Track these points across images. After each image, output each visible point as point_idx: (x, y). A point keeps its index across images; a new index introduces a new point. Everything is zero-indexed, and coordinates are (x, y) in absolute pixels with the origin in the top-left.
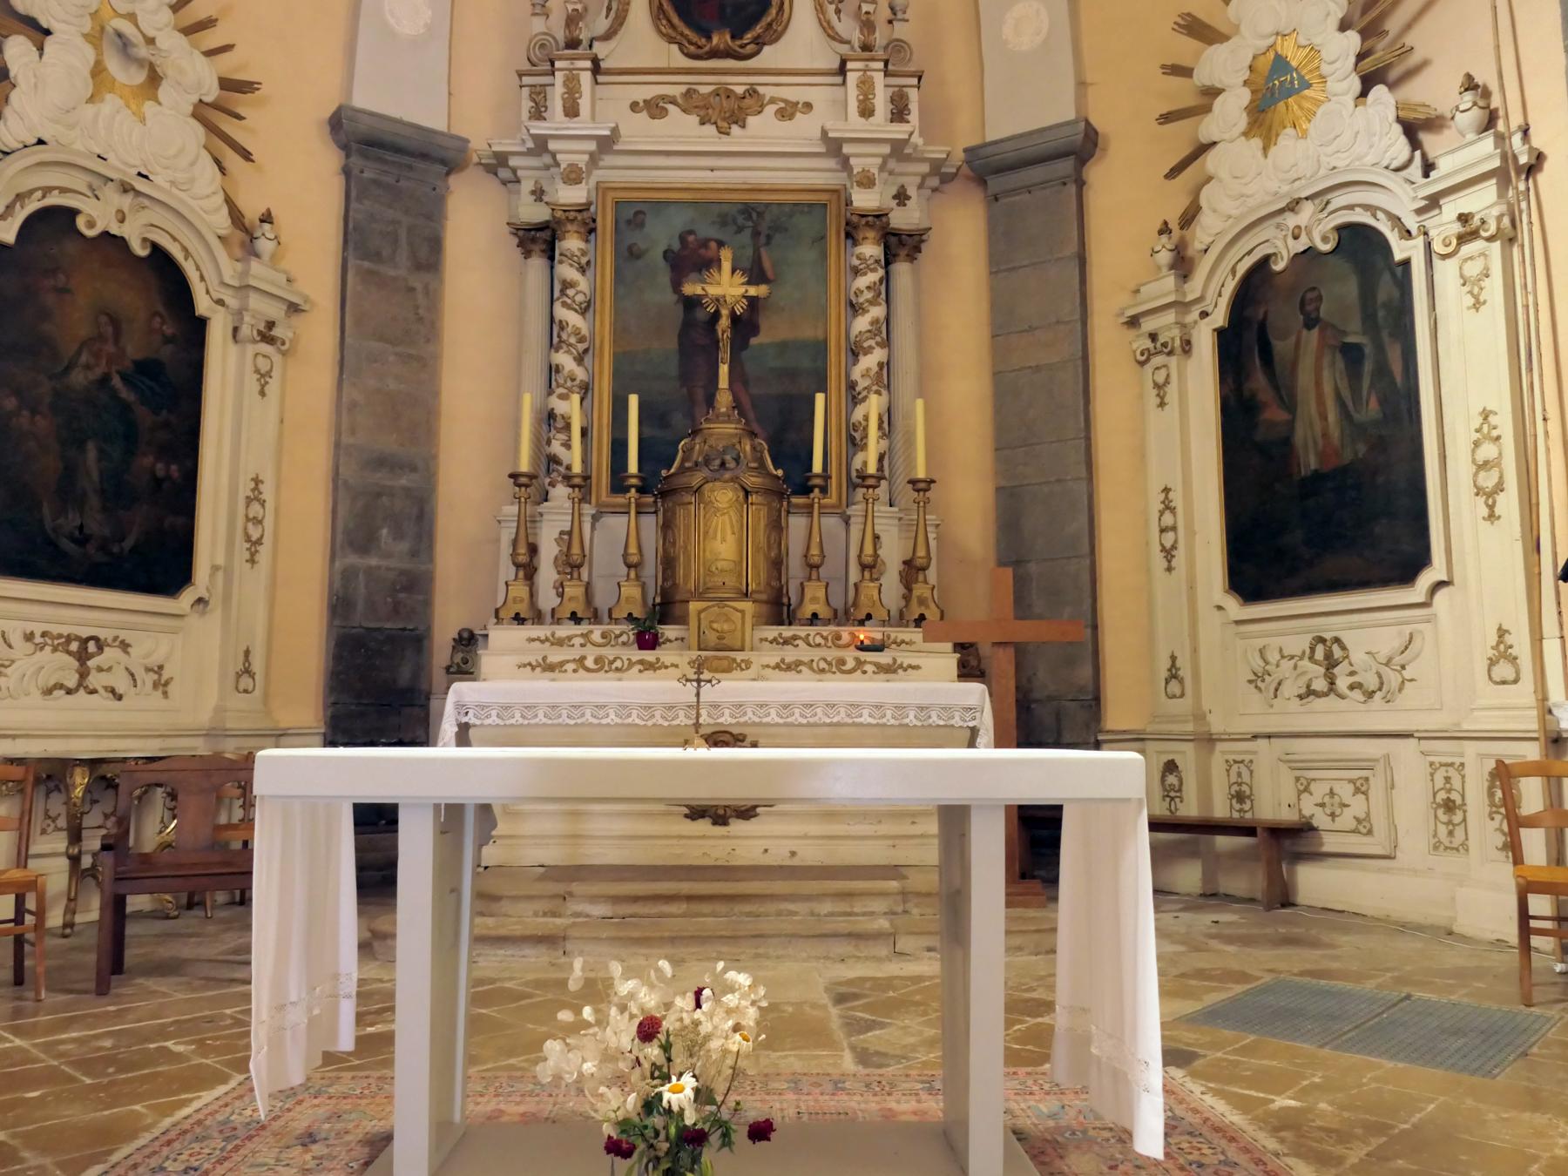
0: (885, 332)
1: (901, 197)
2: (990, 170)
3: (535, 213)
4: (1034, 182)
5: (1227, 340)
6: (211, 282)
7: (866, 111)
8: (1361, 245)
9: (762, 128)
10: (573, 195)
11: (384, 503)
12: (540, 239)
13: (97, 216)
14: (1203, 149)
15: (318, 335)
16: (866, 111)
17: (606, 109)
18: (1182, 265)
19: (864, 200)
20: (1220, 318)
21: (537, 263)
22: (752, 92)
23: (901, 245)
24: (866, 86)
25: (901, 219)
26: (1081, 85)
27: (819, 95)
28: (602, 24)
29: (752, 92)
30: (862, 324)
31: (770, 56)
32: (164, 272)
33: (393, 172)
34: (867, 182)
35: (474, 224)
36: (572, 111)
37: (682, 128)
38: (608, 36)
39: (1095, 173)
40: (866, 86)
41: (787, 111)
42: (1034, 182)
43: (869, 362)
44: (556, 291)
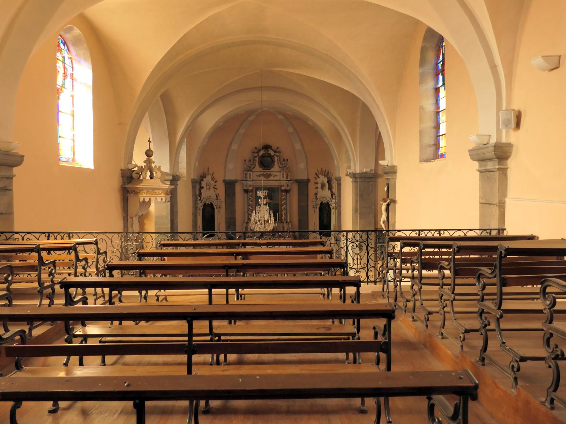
0: (286, 204)
1: (288, 186)
2: (298, 182)
3: (245, 188)
4: (303, 185)
5: (320, 208)
6: (215, 204)
7: (283, 177)
8: (328, 204)
9: (272, 178)
10: (251, 188)
11: (231, 222)
12: (246, 191)
13: (207, 202)
14: (317, 188)
15: (223, 205)
16: (283, 177)
17: (254, 176)
18: (317, 199)
19: (283, 188)
20: (318, 206)
21: (246, 194)
22: (270, 174)
23: (287, 191)
24: (283, 174)
25: (288, 188)
26: (308, 174)
27: (278, 174)
28: (252, 166)
29: (270, 174)
30: (283, 203)
31: (272, 169)
32: (212, 204)
33: (230, 185)
34: (283, 186)
35: (238, 189)
36: (250, 178)
37: (262, 178)
38: (253, 168)
39: (309, 184)
40: (283, 174)
41: (275, 176)
42: (303, 185)
43: (283, 207)
44: (249, 199)
